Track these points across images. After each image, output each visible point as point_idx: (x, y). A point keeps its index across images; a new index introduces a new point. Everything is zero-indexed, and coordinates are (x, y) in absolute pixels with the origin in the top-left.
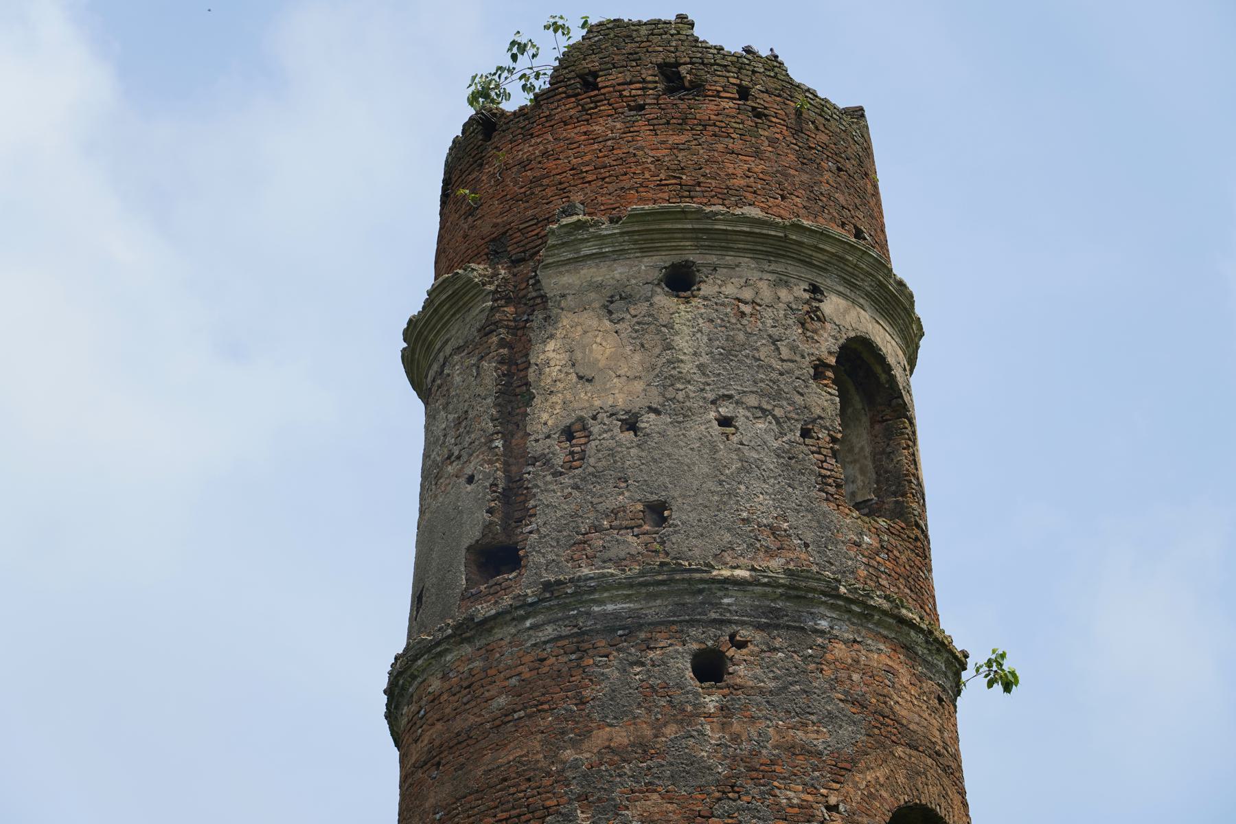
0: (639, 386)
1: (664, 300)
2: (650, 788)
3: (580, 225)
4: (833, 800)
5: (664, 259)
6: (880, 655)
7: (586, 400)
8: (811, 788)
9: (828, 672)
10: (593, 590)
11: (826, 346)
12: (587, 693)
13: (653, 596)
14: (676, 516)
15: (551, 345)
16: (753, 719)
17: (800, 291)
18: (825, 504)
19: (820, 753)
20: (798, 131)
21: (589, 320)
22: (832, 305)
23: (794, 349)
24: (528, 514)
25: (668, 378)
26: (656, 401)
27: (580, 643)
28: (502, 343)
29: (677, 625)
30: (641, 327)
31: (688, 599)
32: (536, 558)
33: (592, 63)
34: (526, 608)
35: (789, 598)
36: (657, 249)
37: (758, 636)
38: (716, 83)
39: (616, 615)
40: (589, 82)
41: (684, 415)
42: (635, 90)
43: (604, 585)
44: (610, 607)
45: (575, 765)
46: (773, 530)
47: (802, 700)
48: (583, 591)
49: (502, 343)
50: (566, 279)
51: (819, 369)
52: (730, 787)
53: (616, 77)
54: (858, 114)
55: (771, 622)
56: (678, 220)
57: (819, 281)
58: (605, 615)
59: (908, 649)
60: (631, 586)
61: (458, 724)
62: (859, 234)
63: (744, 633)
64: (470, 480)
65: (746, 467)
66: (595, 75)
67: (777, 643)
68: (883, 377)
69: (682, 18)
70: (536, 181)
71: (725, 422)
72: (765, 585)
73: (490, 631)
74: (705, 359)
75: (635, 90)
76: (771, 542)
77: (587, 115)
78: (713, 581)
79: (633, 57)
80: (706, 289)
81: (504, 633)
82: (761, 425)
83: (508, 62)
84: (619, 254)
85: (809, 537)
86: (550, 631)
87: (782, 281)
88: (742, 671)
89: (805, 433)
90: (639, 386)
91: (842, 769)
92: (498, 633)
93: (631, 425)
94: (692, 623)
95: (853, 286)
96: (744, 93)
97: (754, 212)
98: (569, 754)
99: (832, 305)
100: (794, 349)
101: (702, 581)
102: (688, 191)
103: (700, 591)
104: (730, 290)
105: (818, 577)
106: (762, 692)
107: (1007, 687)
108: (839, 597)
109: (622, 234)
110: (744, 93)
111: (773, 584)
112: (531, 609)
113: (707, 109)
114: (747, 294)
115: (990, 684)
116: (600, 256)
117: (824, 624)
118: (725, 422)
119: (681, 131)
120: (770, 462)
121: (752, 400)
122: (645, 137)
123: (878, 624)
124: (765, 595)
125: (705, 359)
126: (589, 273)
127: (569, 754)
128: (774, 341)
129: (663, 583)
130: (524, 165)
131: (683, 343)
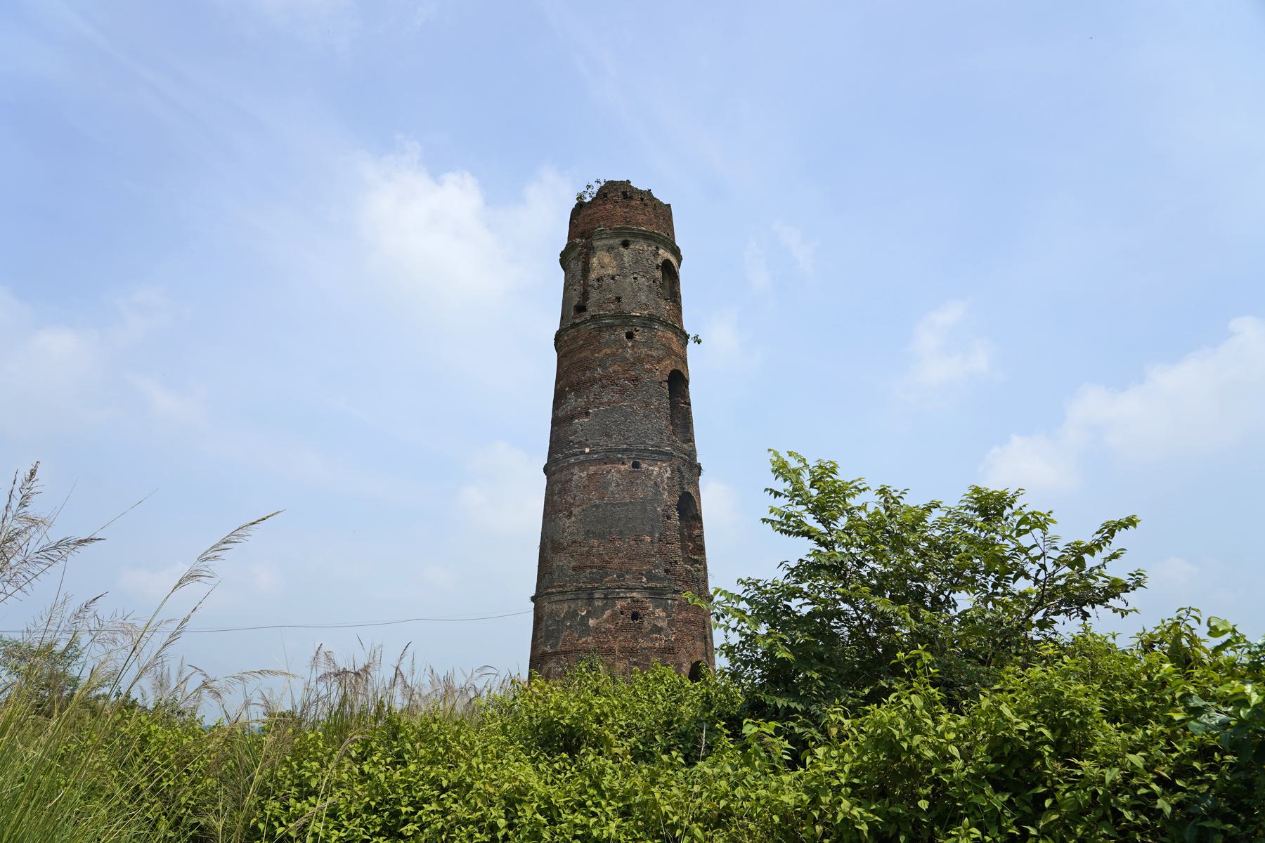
0: (615, 269)
1: (621, 249)
2: (615, 364)
3: (602, 230)
4: (657, 368)
5: (622, 239)
6: (669, 334)
7: (603, 272)
8: (652, 365)
11: (659, 261)
12: (601, 341)
14: (623, 300)
15: (595, 259)
16: (639, 348)
17: (654, 248)
18: (658, 299)
20: (655, 209)
21: (604, 253)
22: (661, 251)
23: (652, 261)
24: (589, 299)
25: (622, 267)
27: (599, 329)
28: (583, 258)
29: (622, 326)
30: (616, 255)
32: (590, 309)
33: (606, 191)
34: (587, 321)
35: (648, 320)
37: (641, 329)
40: (605, 195)
41: (625, 276)
42: (616, 198)
43: (606, 316)
45: (598, 358)
46: (645, 304)
47: (651, 344)
48: (601, 317)
49: (583, 258)
50: (598, 243)
51: (658, 267)
52: (633, 364)
53: (612, 194)
54: (669, 205)
55: (644, 326)
58: (606, 323)
59: (676, 334)
61: (571, 347)
62: (668, 235)
64: (575, 290)
65: (640, 289)
66: (607, 194)
69: (628, 181)
70: (592, 219)
71: (635, 278)
74: (631, 263)
75: (616, 198)
76: (644, 307)
77: (605, 204)
79: (616, 190)
80: (631, 247)
81: (582, 326)
82: (644, 280)
83: (586, 190)
85: (654, 306)
86: (593, 326)
87: (649, 245)
89: (654, 282)
90: (615, 269)
91: (659, 361)
92: (581, 326)
93: (613, 278)
94: (626, 325)
95: (666, 247)
96: (642, 199)
97: (644, 229)
98: (596, 355)
100: (652, 261)
102: (628, 223)
104: (637, 247)
105: (656, 316)
107: (699, 343)
110: (642, 199)
111: (645, 317)
112: (588, 321)
113: (633, 203)
114: (641, 248)
116: (607, 238)
117: (657, 327)
118: (635, 278)
119: (627, 208)
120: (645, 289)
121: (642, 274)
122: (618, 209)
125: (631, 263)
126: (604, 242)
127: (596, 355)
128: (647, 260)
130: (589, 215)
131: (625, 259)
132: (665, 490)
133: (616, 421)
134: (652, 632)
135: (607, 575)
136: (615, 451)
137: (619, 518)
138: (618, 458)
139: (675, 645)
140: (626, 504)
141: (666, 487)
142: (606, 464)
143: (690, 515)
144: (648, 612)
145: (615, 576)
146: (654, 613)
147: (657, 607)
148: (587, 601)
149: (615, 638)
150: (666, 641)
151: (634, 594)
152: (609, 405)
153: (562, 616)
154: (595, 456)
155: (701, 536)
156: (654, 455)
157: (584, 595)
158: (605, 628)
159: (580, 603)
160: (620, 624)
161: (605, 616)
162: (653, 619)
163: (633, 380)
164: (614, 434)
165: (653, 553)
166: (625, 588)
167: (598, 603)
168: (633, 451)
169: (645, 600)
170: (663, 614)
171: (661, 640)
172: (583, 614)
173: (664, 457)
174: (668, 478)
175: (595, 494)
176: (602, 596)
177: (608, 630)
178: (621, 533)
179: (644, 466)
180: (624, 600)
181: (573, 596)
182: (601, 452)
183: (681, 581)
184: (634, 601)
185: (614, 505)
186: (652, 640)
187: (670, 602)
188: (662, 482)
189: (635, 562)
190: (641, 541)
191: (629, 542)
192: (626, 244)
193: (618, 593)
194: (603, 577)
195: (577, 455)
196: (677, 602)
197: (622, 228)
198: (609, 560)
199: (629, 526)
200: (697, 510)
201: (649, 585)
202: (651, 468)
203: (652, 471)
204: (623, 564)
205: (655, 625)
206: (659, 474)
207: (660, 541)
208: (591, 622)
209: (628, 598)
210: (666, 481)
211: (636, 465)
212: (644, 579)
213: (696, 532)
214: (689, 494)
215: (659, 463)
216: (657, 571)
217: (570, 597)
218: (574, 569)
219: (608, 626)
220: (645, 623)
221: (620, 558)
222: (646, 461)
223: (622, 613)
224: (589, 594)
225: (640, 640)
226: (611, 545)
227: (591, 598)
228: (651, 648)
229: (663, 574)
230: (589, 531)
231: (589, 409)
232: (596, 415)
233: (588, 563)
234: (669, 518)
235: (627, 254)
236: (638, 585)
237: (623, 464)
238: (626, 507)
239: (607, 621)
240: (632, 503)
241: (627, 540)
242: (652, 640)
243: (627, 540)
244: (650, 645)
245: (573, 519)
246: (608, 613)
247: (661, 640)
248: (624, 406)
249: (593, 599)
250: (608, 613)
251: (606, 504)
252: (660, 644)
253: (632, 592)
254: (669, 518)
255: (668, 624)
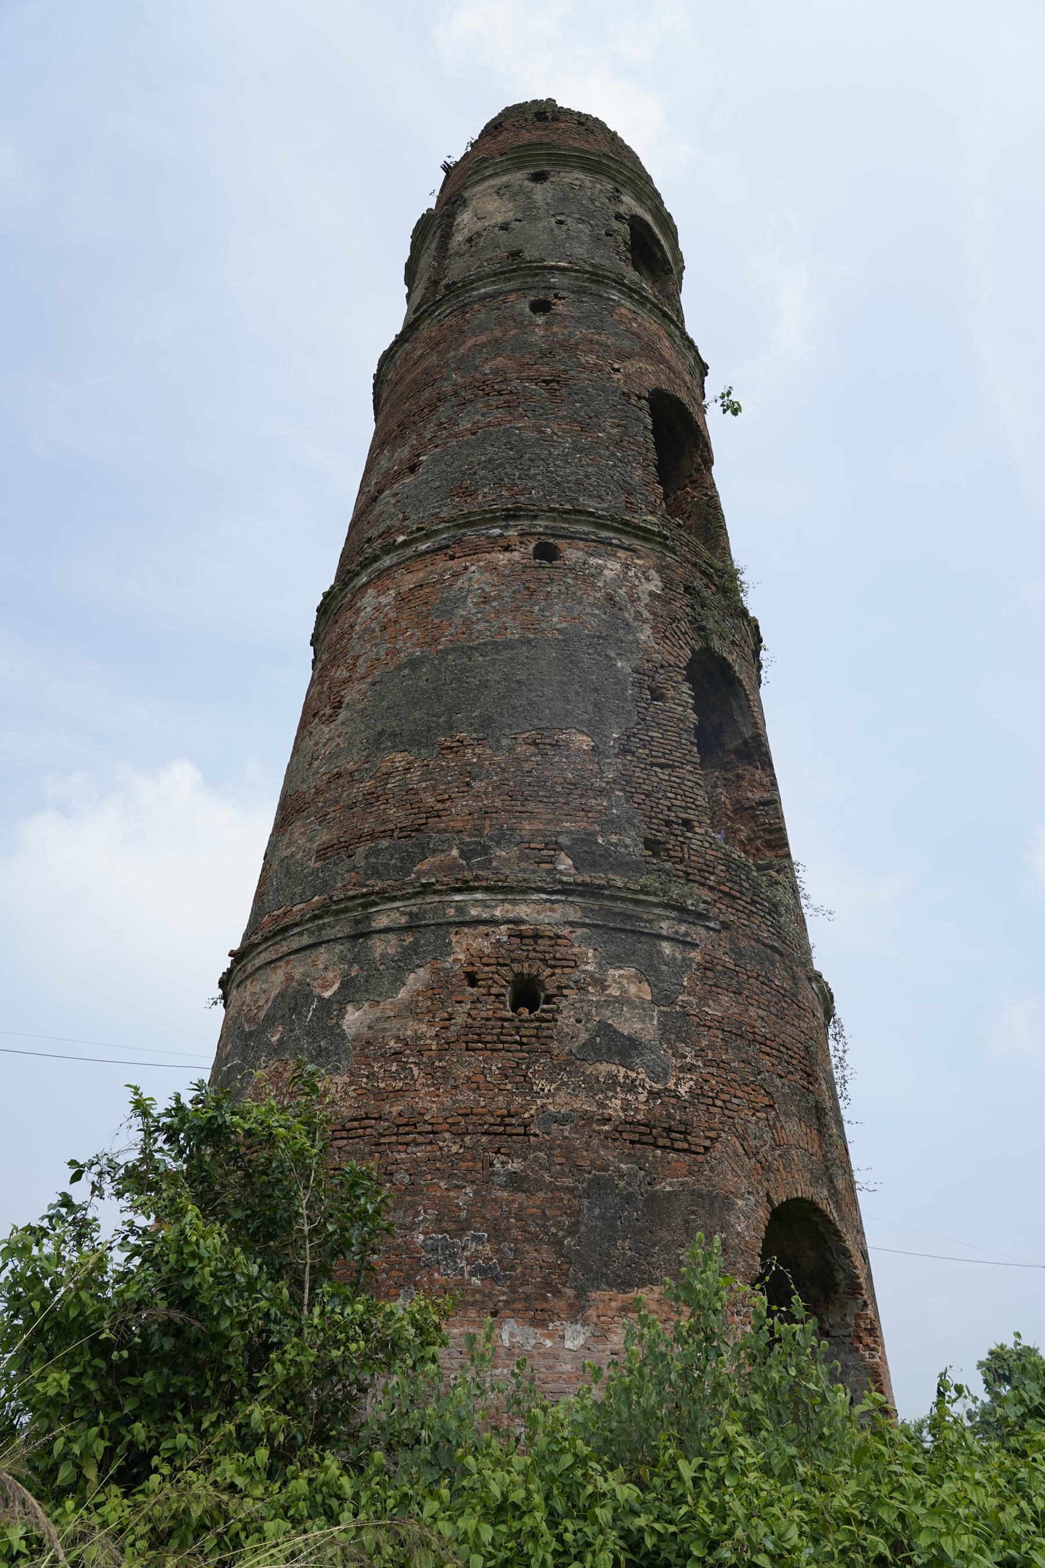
4: (616, 366)
9: (616, 317)
10: (473, 282)
13: (507, 280)
19: (609, 347)
26: (519, 216)
31: (529, 279)
35: (592, 281)
36: (526, 167)
38: (563, 118)
39: (485, 293)
44: (483, 291)
56: (539, 149)
57: (620, 188)
60: (495, 275)
63: (562, 294)
67: (584, 299)
68: (659, 254)
72: (577, 271)
73: (417, 329)
78: (545, 267)
80: (552, 179)
84: (506, 171)
88: (560, 308)
92: (421, 327)
99: (626, 199)
101: (537, 267)
103: (537, 275)
106: (572, 317)
107: (735, 412)
108: (624, 285)
109: (507, 160)
115: (724, 411)
116: (495, 175)
118: (560, 222)
123: (650, 311)
124: (577, 278)
129: (513, 270)
132: (645, 621)
133: (490, 460)
134: (593, 1051)
135: (425, 851)
136: (484, 521)
137: (485, 685)
138: (489, 537)
139: (698, 1117)
140: (508, 645)
141: (646, 614)
142: (452, 558)
143: (735, 743)
144: (576, 975)
145: (455, 852)
146: (602, 984)
147: (615, 960)
148: (348, 945)
149: (438, 1076)
150: (653, 1094)
151: (523, 911)
152: (474, 434)
153: (262, 1015)
154: (424, 547)
155: (773, 804)
156: (604, 534)
157: (343, 929)
158: (398, 1039)
159: (322, 956)
160: (459, 1020)
161: (403, 994)
162: (598, 1005)
163: (547, 382)
164: (484, 486)
165: (597, 783)
166: (488, 889)
167: (382, 947)
168: (535, 517)
169: (565, 931)
170: (641, 991)
171: (631, 1087)
172: (327, 994)
173: (636, 544)
174: (651, 594)
175: (413, 634)
176: (403, 920)
177: (414, 1045)
178: (486, 722)
179: (572, 554)
180: (482, 929)
181: (306, 940)
182: (436, 532)
183: (711, 888)
184: (521, 936)
185: (467, 651)
186: (592, 1085)
187: (667, 948)
188: (633, 600)
189: (531, 806)
190: (556, 745)
191: (511, 749)
192: (539, 177)
193: (461, 909)
194: (409, 861)
195: (376, 558)
196: (696, 955)
197: (530, 145)
198: (440, 806)
199: (515, 702)
200: (755, 725)
201: (579, 879)
202: (593, 561)
203: (600, 569)
204: (486, 813)
205: (604, 1028)
206: (622, 579)
207: (625, 751)
208: (353, 1019)
209: (494, 922)
210: (646, 600)
211: (547, 553)
212: (565, 863)
213: (757, 795)
214: (725, 667)
215: (621, 554)
216: (614, 839)
217: (296, 943)
218: (322, 854)
219: (412, 1028)
220: (566, 1019)
221: (477, 797)
222: (581, 543)
223: (472, 980)
224: (357, 922)
225: (539, 1084)
226: (451, 761)
227: (361, 934)
228: (588, 1119)
229: (639, 851)
230: (381, 733)
231: (418, 456)
232: (435, 461)
233: (366, 828)
234: (657, 695)
235: (540, 193)
236: (539, 876)
237: (507, 549)
238: (507, 654)
239: (411, 1010)
240: (529, 641)
241: (505, 742)
242: (592, 1085)
243: (505, 742)
244: (584, 1104)
245: (343, 714)
246: (417, 979)
247: (631, 1087)
248: (519, 429)
249: (367, 935)
250: (417, 979)
251: (446, 652)
252: (626, 1106)
253: (514, 903)
254: (657, 695)
255: (663, 1026)
